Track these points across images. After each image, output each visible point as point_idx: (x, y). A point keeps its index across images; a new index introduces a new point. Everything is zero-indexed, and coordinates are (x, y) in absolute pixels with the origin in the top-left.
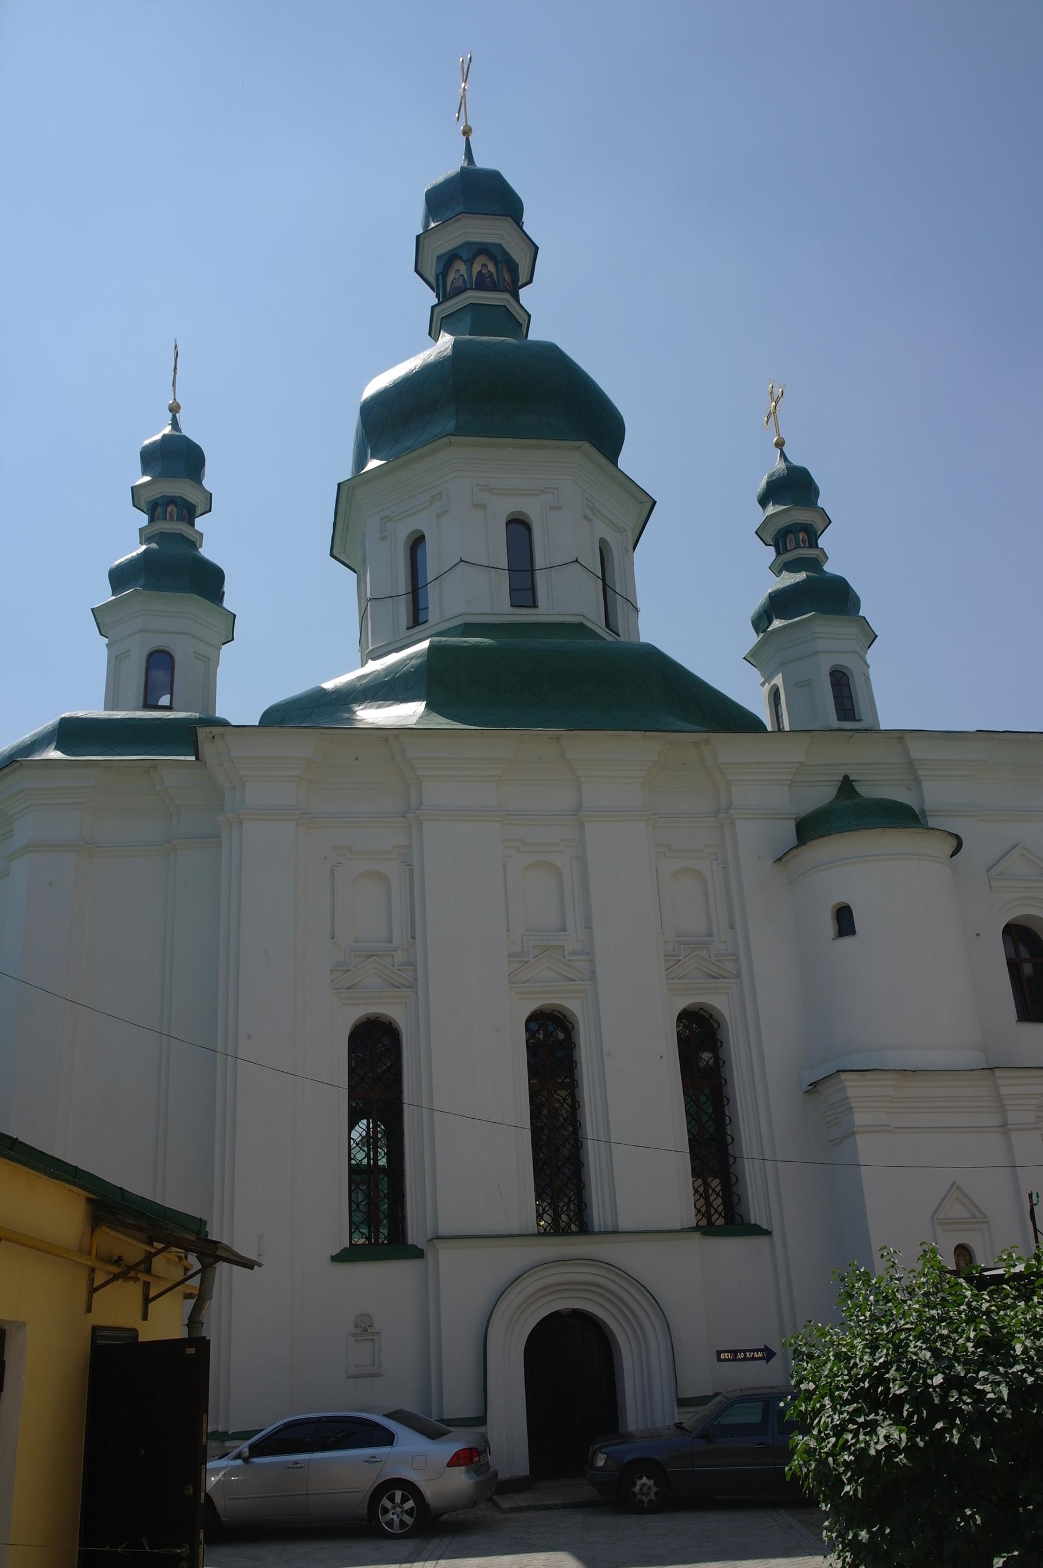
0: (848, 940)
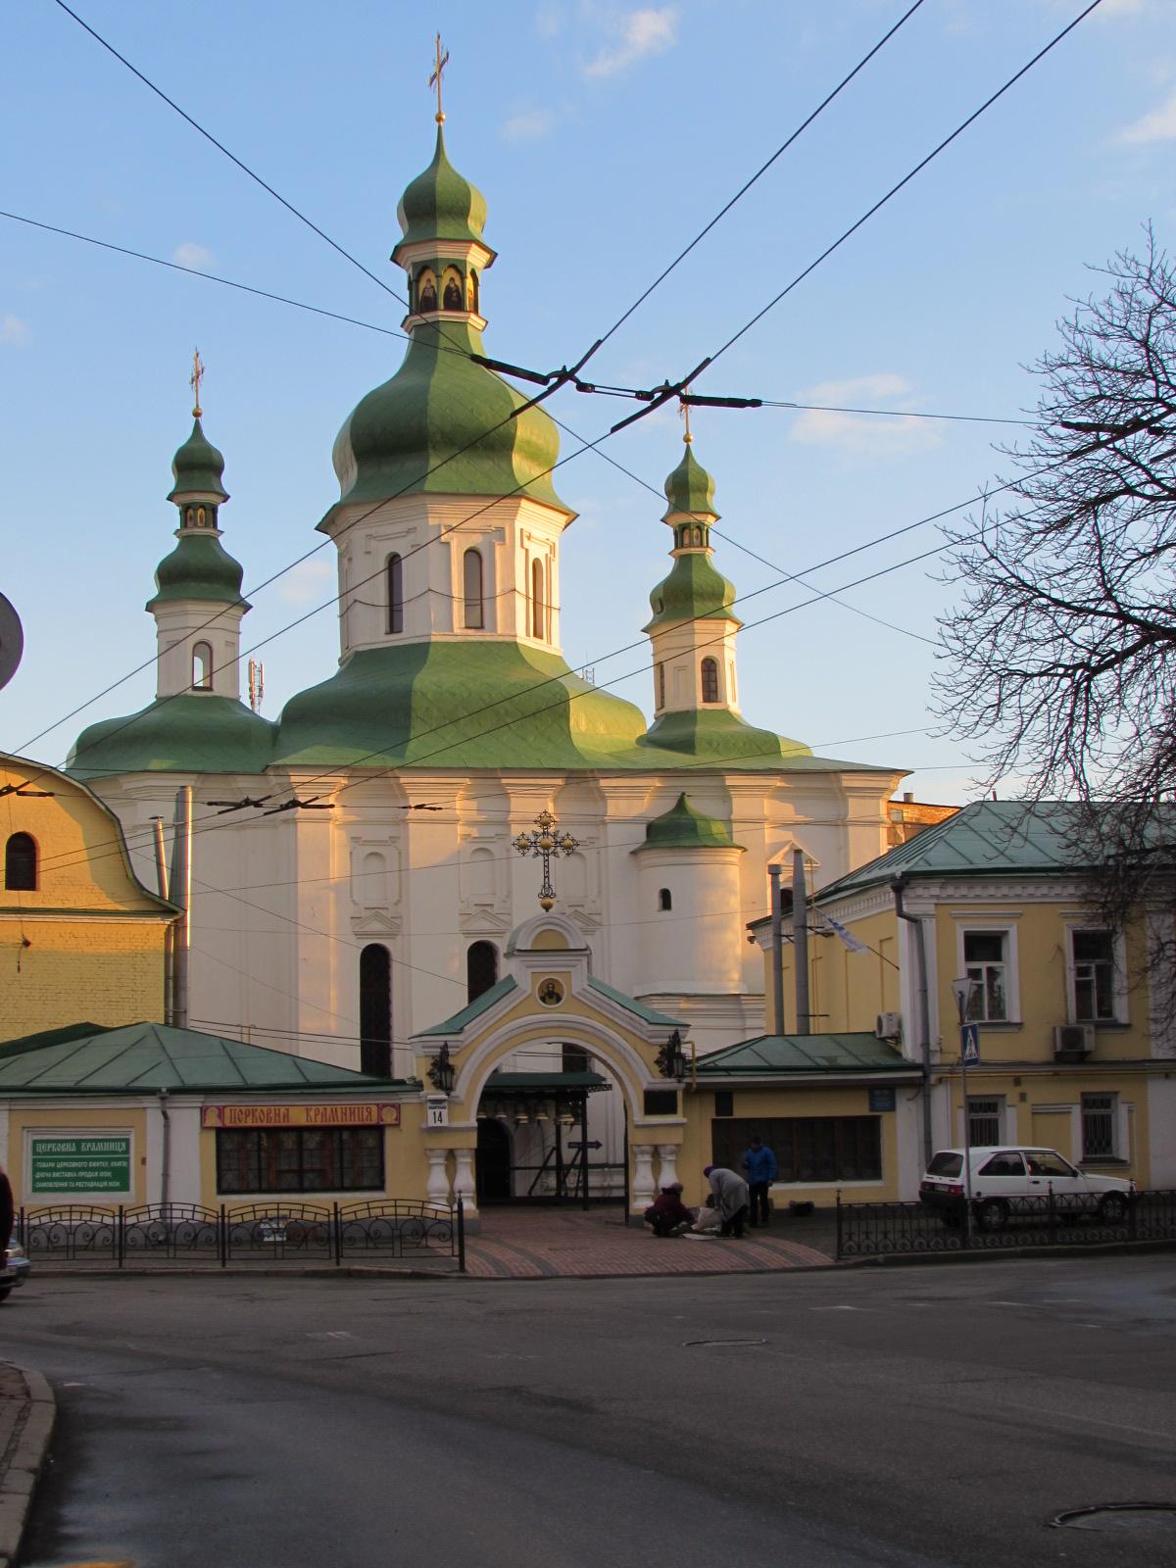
0: (666, 913)
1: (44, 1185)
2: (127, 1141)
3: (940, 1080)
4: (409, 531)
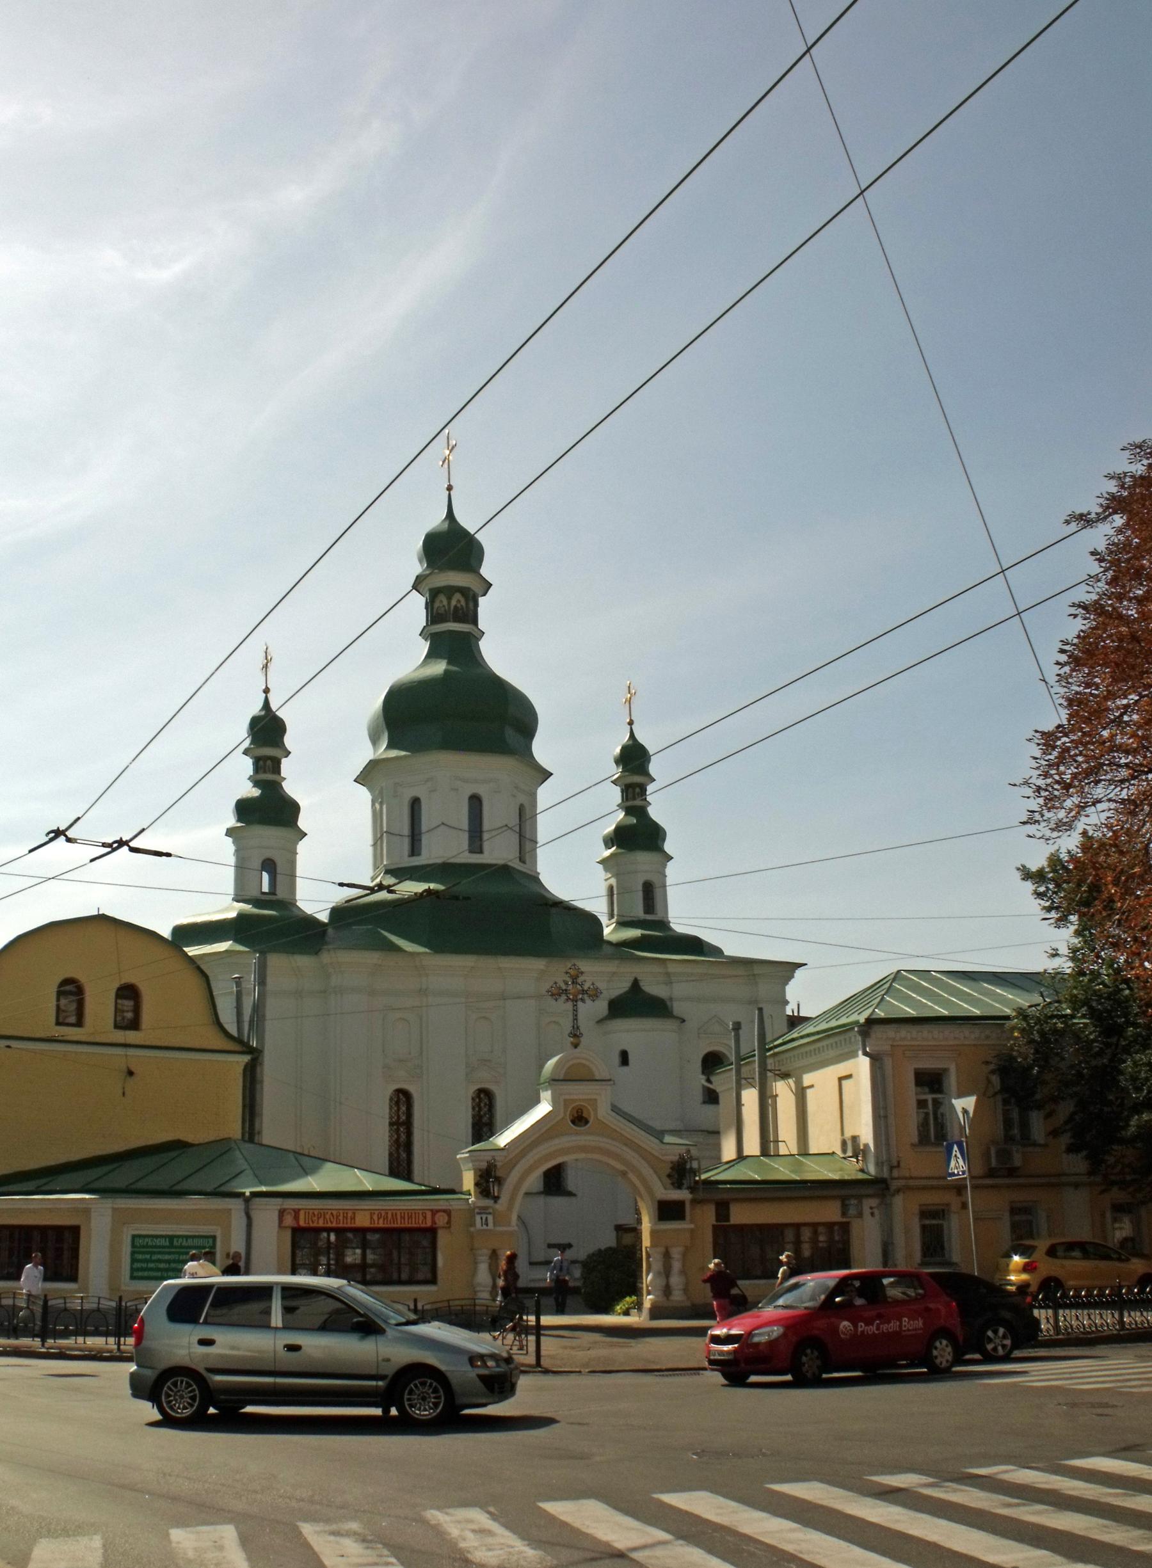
0: (625, 1069)
1: (140, 1274)
2: (214, 1238)
3: (898, 1191)
4: (427, 780)
